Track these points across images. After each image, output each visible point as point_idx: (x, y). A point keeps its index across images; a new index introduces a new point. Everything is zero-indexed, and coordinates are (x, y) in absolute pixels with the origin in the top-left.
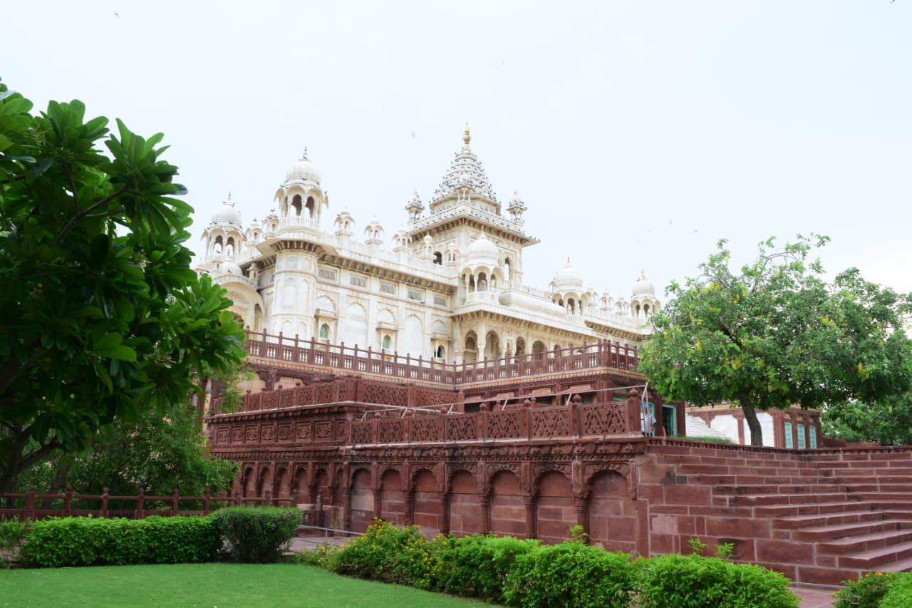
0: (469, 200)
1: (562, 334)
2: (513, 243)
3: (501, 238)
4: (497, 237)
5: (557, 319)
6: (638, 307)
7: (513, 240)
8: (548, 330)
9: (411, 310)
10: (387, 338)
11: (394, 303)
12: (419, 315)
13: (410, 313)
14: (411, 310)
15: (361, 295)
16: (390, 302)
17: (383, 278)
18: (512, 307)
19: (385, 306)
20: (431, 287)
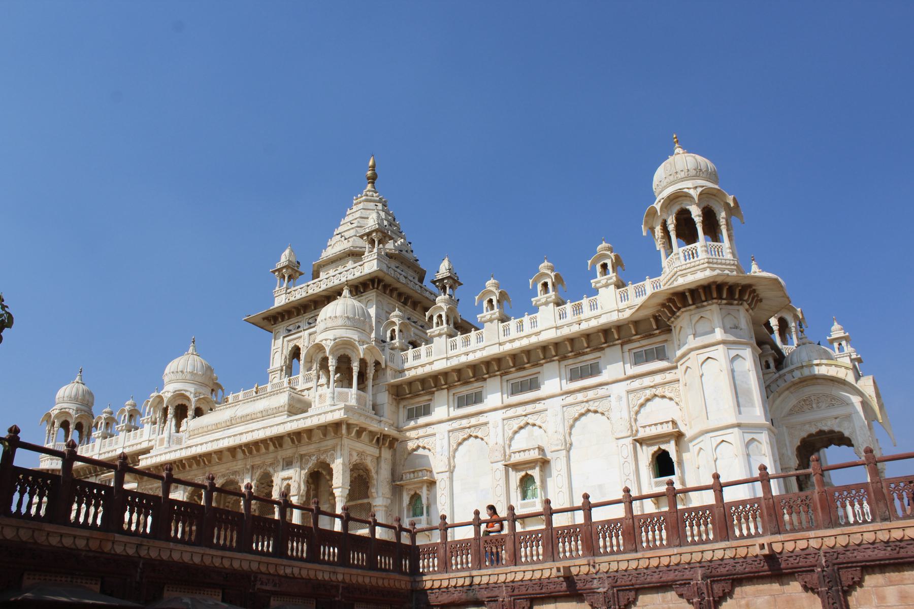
1: (267, 448)
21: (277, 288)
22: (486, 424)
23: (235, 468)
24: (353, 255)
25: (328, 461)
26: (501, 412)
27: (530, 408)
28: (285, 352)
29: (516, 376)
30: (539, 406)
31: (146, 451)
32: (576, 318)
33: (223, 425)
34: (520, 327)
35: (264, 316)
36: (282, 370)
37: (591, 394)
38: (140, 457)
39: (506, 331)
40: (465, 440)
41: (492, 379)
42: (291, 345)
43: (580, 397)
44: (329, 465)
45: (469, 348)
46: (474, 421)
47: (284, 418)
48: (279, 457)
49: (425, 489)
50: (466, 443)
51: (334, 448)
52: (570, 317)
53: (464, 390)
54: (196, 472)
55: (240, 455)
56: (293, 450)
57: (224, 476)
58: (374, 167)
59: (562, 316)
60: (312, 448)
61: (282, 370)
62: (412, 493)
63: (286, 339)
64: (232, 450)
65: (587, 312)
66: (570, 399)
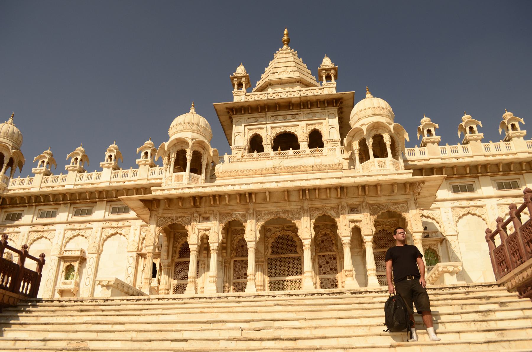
3: (295, 111)
4: (289, 112)
5: (330, 175)
7: (318, 107)
8: (294, 197)
9: (113, 228)
10: (69, 270)
11: (89, 226)
12: (123, 231)
13: (111, 231)
14: (113, 228)
15: (46, 228)
16: (83, 226)
17: (76, 203)
18: (217, 182)
19: (75, 233)
21: (235, 90)
22: (482, 206)
23: (288, 208)
24: (301, 83)
25: (398, 210)
26: (495, 200)
28: (246, 136)
29: (501, 178)
31: (160, 185)
33: (264, 172)
35: (228, 106)
36: (245, 149)
38: (152, 188)
39: (487, 148)
40: (464, 215)
41: (483, 177)
42: (251, 133)
44: (400, 215)
46: (472, 203)
48: (343, 203)
49: (439, 245)
50: (464, 217)
51: (406, 202)
53: (458, 182)
54: (235, 207)
55: (294, 197)
56: (361, 199)
57: (271, 213)
58: (288, 34)
61: (245, 149)
62: (427, 248)
63: (246, 127)
64: (288, 192)
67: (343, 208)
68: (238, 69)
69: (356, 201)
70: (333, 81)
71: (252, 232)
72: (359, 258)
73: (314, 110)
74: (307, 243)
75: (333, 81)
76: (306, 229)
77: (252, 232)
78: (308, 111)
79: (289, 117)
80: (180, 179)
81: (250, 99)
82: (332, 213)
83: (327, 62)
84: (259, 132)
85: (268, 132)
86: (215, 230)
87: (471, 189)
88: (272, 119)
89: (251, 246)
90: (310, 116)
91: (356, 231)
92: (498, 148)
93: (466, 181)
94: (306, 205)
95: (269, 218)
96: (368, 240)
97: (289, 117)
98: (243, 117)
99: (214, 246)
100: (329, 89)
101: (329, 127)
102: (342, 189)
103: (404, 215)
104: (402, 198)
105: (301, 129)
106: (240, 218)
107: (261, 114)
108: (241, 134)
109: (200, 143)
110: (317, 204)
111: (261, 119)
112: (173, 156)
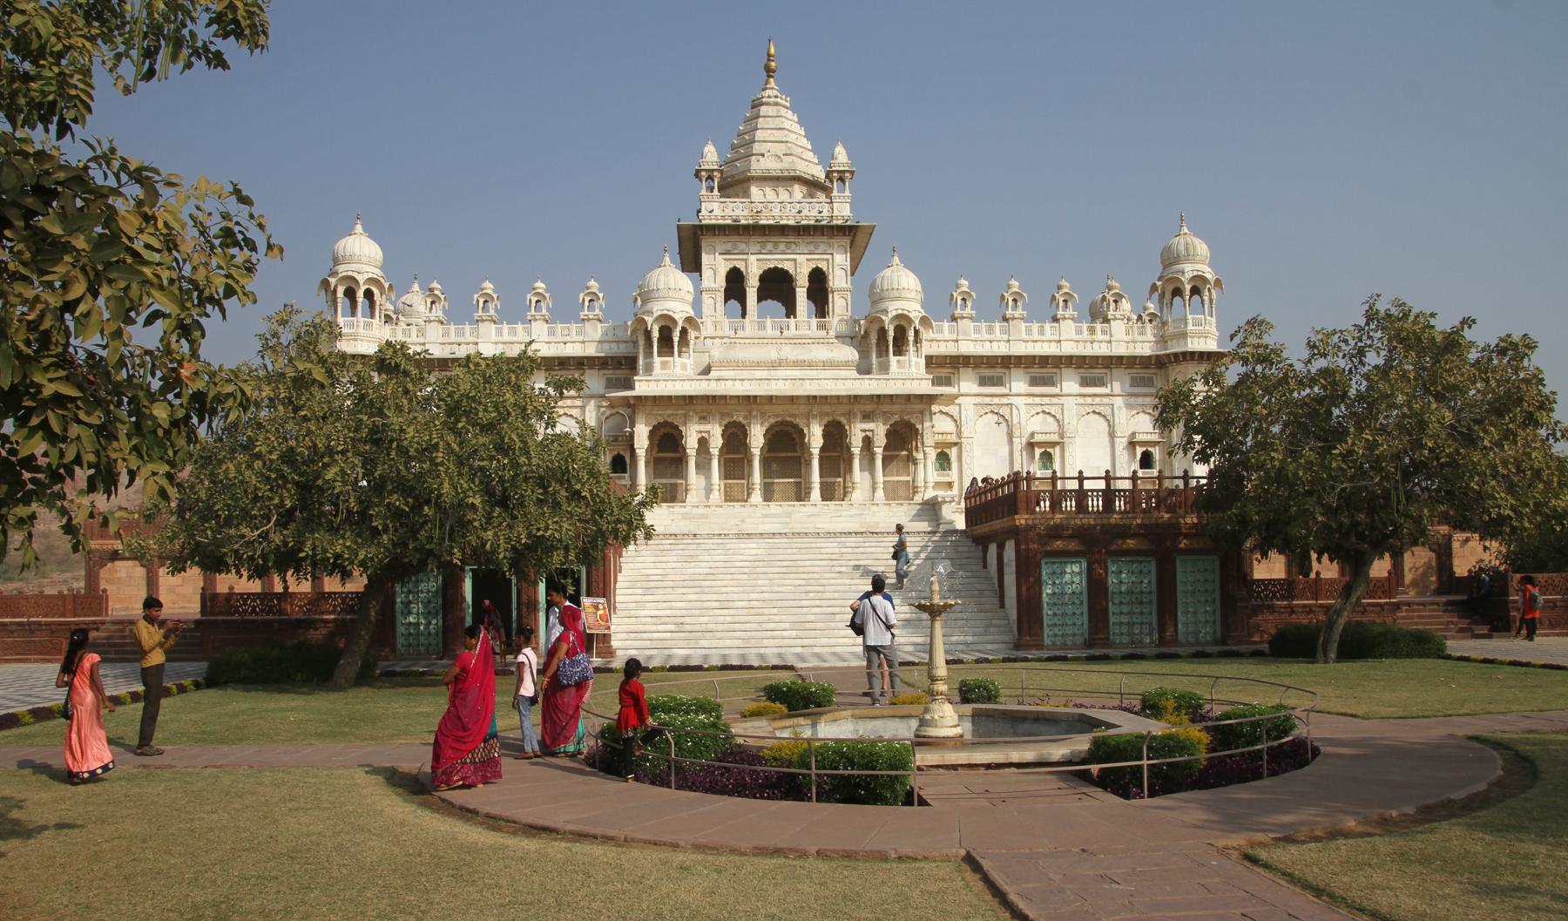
0: (716, 191)
2: (825, 239)
6: (1195, 291)
18: (713, 374)
20: (592, 367)
27: (1046, 400)
30: (1055, 400)
32: (1090, 338)
34: (1042, 332)
37: (1097, 400)
42: (730, 265)
43: (1089, 400)
45: (992, 337)
46: (996, 400)
47: (854, 374)
51: (922, 413)
52: (1085, 335)
53: (987, 372)
59: (1079, 331)
60: (896, 408)
65: (1099, 336)
66: (1081, 400)
67: (855, 416)
68: (706, 150)
69: (869, 408)
70: (847, 193)
71: (757, 438)
72: (866, 462)
73: (818, 239)
74: (816, 452)
75: (847, 193)
76: (815, 437)
77: (757, 438)
78: (810, 239)
79: (782, 247)
80: (664, 365)
81: (728, 212)
82: (843, 420)
83: (841, 157)
84: (741, 266)
85: (754, 269)
86: (716, 435)
87: (999, 382)
88: (758, 247)
89: (756, 452)
90: (811, 247)
91: (868, 443)
92: (1042, 332)
93: (998, 371)
94: (816, 409)
95: (772, 421)
96: (879, 451)
97: (782, 247)
98: (721, 243)
99: (715, 452)
100: (842, 209)
101: (837, 264)
102: (856, 399)
103: (919, 426)
104: (919, 407)
105: (799, 265)
106: (741, 419)
107: (744, 238)
108: (716, 266)
109: (689, 320)
110: (827, 409)
111: (742, 246)
112: (656, 334)
